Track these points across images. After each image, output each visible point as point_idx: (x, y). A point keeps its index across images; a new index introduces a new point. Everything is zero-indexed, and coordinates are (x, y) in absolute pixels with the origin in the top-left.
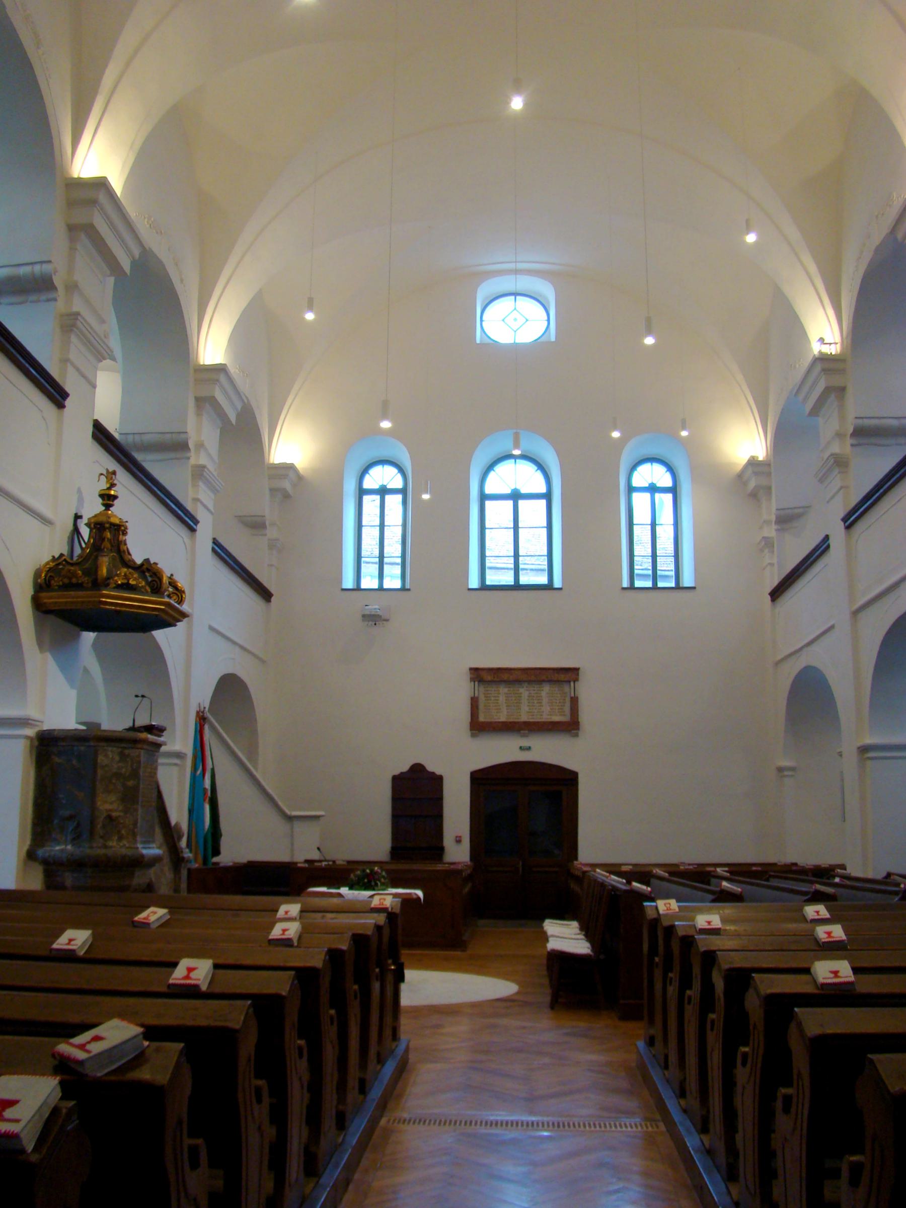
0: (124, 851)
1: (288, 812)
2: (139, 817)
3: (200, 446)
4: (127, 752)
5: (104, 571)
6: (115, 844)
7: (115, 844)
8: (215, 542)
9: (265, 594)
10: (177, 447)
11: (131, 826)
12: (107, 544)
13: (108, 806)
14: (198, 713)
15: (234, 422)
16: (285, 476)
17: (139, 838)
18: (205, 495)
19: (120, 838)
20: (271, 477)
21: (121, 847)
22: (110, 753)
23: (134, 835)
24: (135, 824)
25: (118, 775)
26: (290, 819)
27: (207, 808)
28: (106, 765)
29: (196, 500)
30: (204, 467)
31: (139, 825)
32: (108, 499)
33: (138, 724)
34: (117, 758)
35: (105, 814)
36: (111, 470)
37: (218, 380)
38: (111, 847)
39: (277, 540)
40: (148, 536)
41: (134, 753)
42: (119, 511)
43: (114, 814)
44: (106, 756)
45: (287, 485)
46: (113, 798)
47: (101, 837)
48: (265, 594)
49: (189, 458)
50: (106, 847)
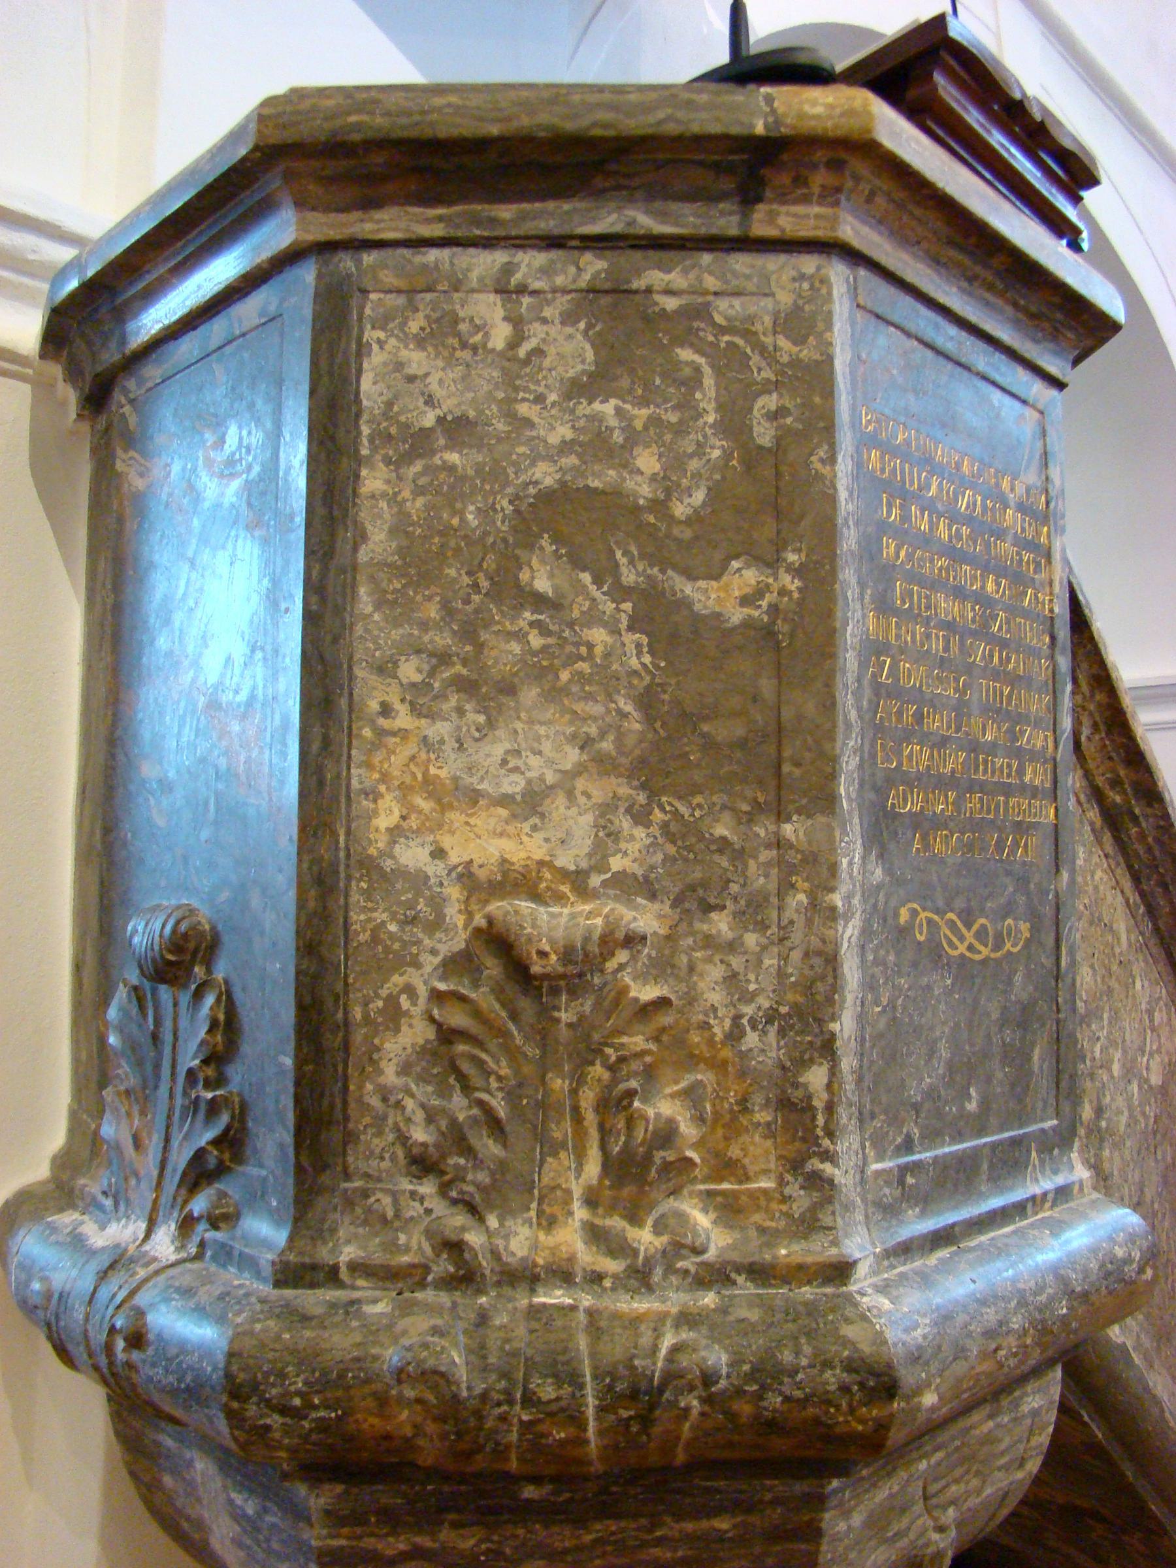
2: (849, 932)
4: (667, 282)
6: (569, 1238)
7: (569, 1238)
11: (763, 1047)
13: (485, 842)
17: (853, 1162)
19: (637, 1173)
21: (640, 1277)
23: (802, 1130)
24: (805, 1018)
25: (572, 517)
28: (457, 428)
31: (845, 1026)
34: (569, 349)
38: (526, 1276)
43: (548, 926)
44: (446, 333)
46: (539, 745)
47: (422, 1164)
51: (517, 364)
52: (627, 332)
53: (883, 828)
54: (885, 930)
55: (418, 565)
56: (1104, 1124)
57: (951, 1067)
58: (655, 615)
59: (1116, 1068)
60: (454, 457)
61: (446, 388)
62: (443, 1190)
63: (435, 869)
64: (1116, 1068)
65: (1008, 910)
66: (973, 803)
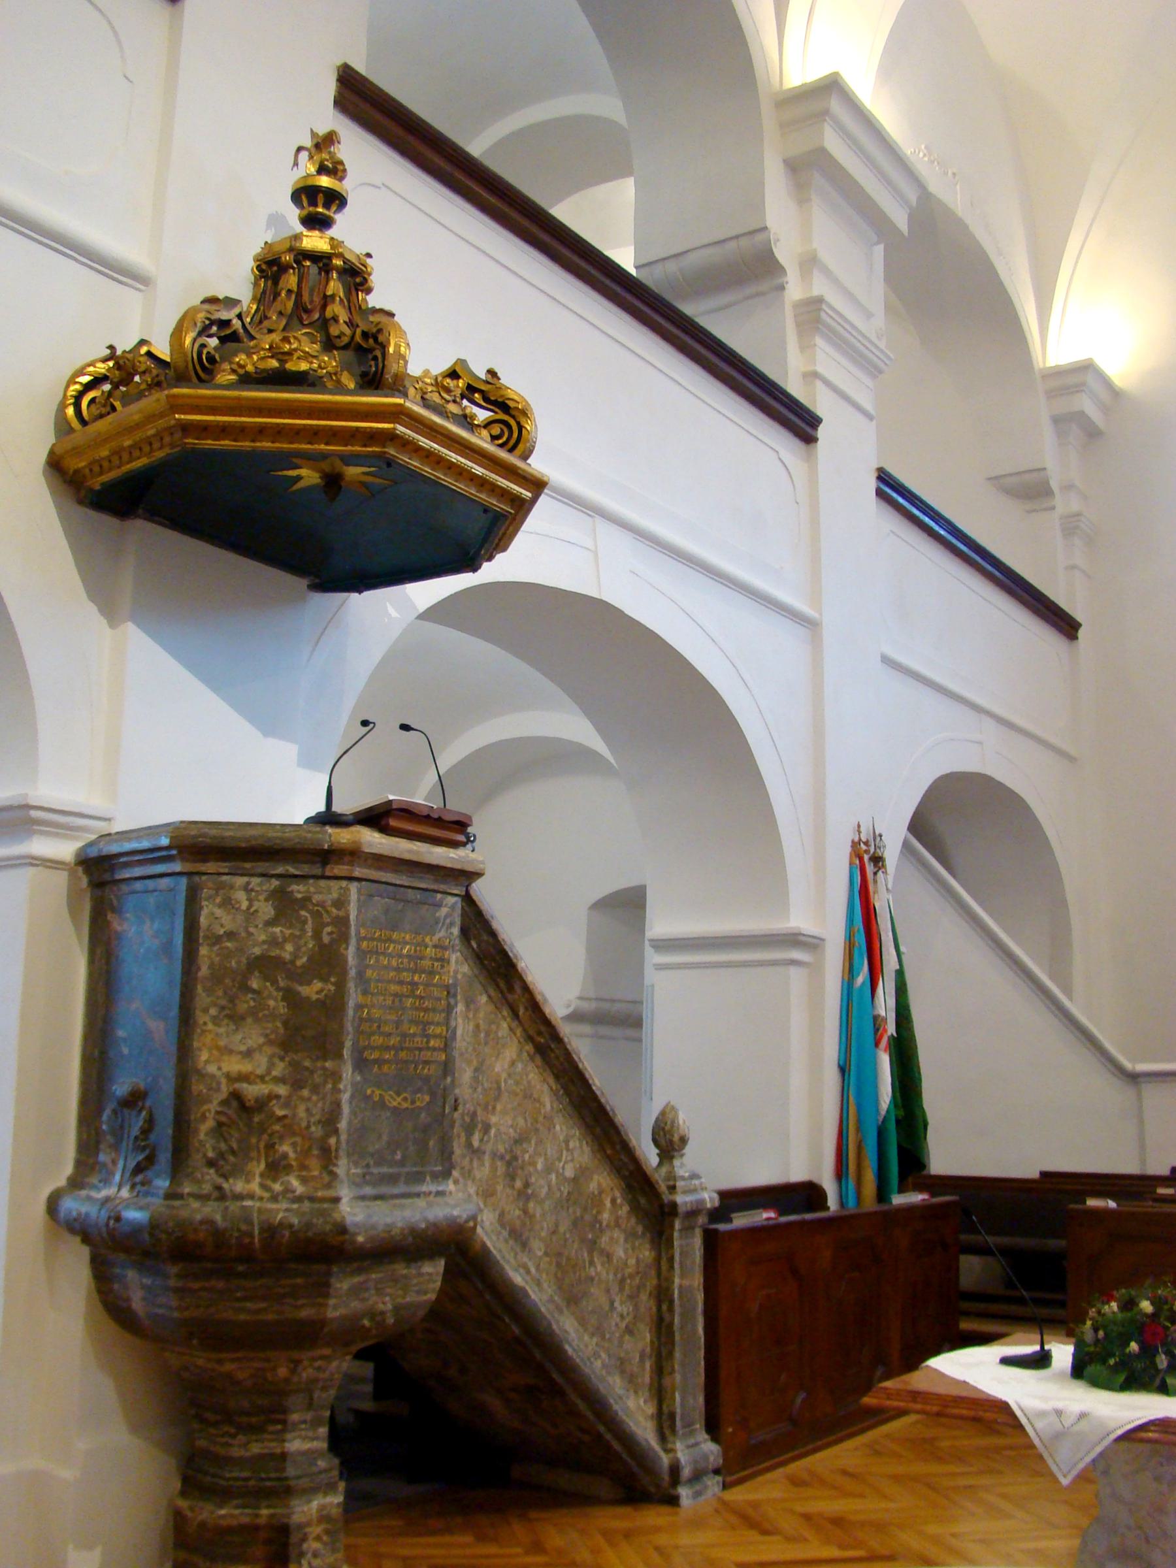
0: (281, 1211)
1: (1128, 1065)
2: (345, 1097)
4: (298, 890)
6: (255, 1186)
7: (255, 1186)
8: (884, 477)
9: (1065, 625)
10: (754, 268)
11: (317, 1131)
13: (235, 1066)
14: (855, 845)
15: (906, 232)
16: (1079, 388)
17: (342, 1167)
18: (828, 360)
19: (276, 1168)
20: (1051, 394)
21: (274, 1198)
22: (241, 896)
23: (328, 1157)
24: (330, 1122)
25: (266, 965)
26: (1134, 1078)
27: (885, 1061)
28: (231, 935)
29: (812, 376)
30: (820, 300)
31: (343, 1125)
32: (318, 202)
33: (345, 805)
34: (266, 910)
35: (225, 1090)
36: (322, 131)
37: (826, 112)
38: (239, 1197)
39: (1079, 514)
40: (445, 294)
41: (325, 892)
42: (350, 232)
43: (252, 1091)
46: (252, 1036)
47: (211, 1163)
48: (1065, 625)
49: (782, 288)
50: (221, 1195)
51: (250, 915)
52: (285, 906)
53: (361, 1064)
54: (359, 1095)
55: (217, 977)
56: (530, 1191)
57: (389, 1143)
58: (290, 997)
59: (540, 1166)
60: (229, 944)
62: (217, 1171)
63: (218, 1073)
64: (540, 1166)
65: (419, 1090)
66: (403, 1055)
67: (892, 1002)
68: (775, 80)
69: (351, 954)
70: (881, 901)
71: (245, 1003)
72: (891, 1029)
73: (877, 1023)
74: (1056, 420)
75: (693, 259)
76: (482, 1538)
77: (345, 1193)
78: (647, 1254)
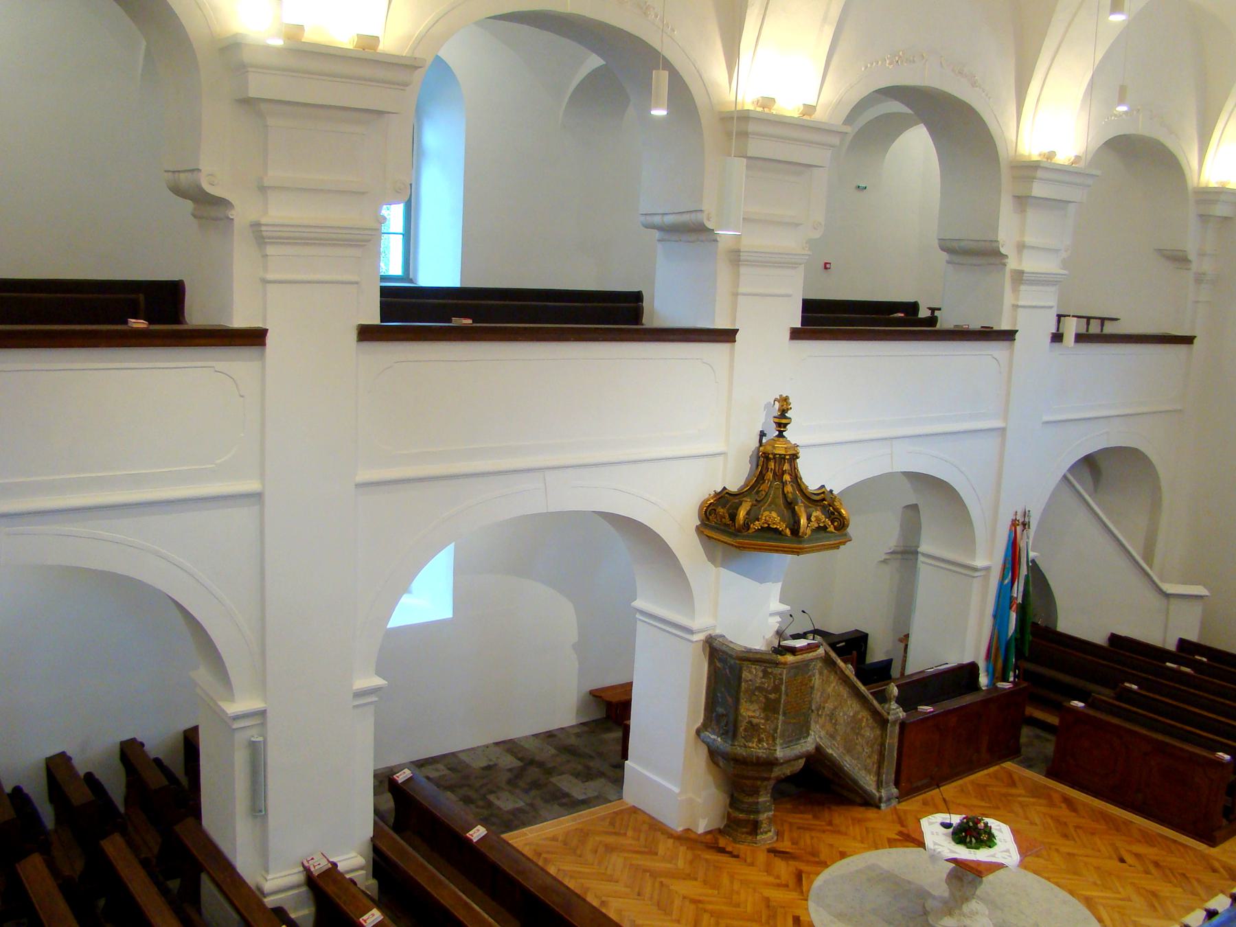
3: (1021, 247)
5: (742, 514)
12: (770, 475)
13: (751, 714)
17: (778, 741)
19: (760, 741)
23: (774, 739)
24: (775, 730)
25: (760, 689)
27: (1013, 616)
34: (761, 674)
41: (777, 671)
43: (755, 721)
44: (750, 672)
45: (1220, 210)
49: (1005, 265)
53: (784, 714)
54: (784, 722)
55: (746, 691)
58: (766, 698)
61: (750, 677)
67: (1021, 589)
68: (1011, 152)
69: (783, 688)
70: (1022, 544)
71: (754, 698)
72: (1020, 600)
73: (1012, 599)
74: (1201, 216)
75: (962, 244)
76: (815, 817)
77: (778, 748)
78: (878, 732)
